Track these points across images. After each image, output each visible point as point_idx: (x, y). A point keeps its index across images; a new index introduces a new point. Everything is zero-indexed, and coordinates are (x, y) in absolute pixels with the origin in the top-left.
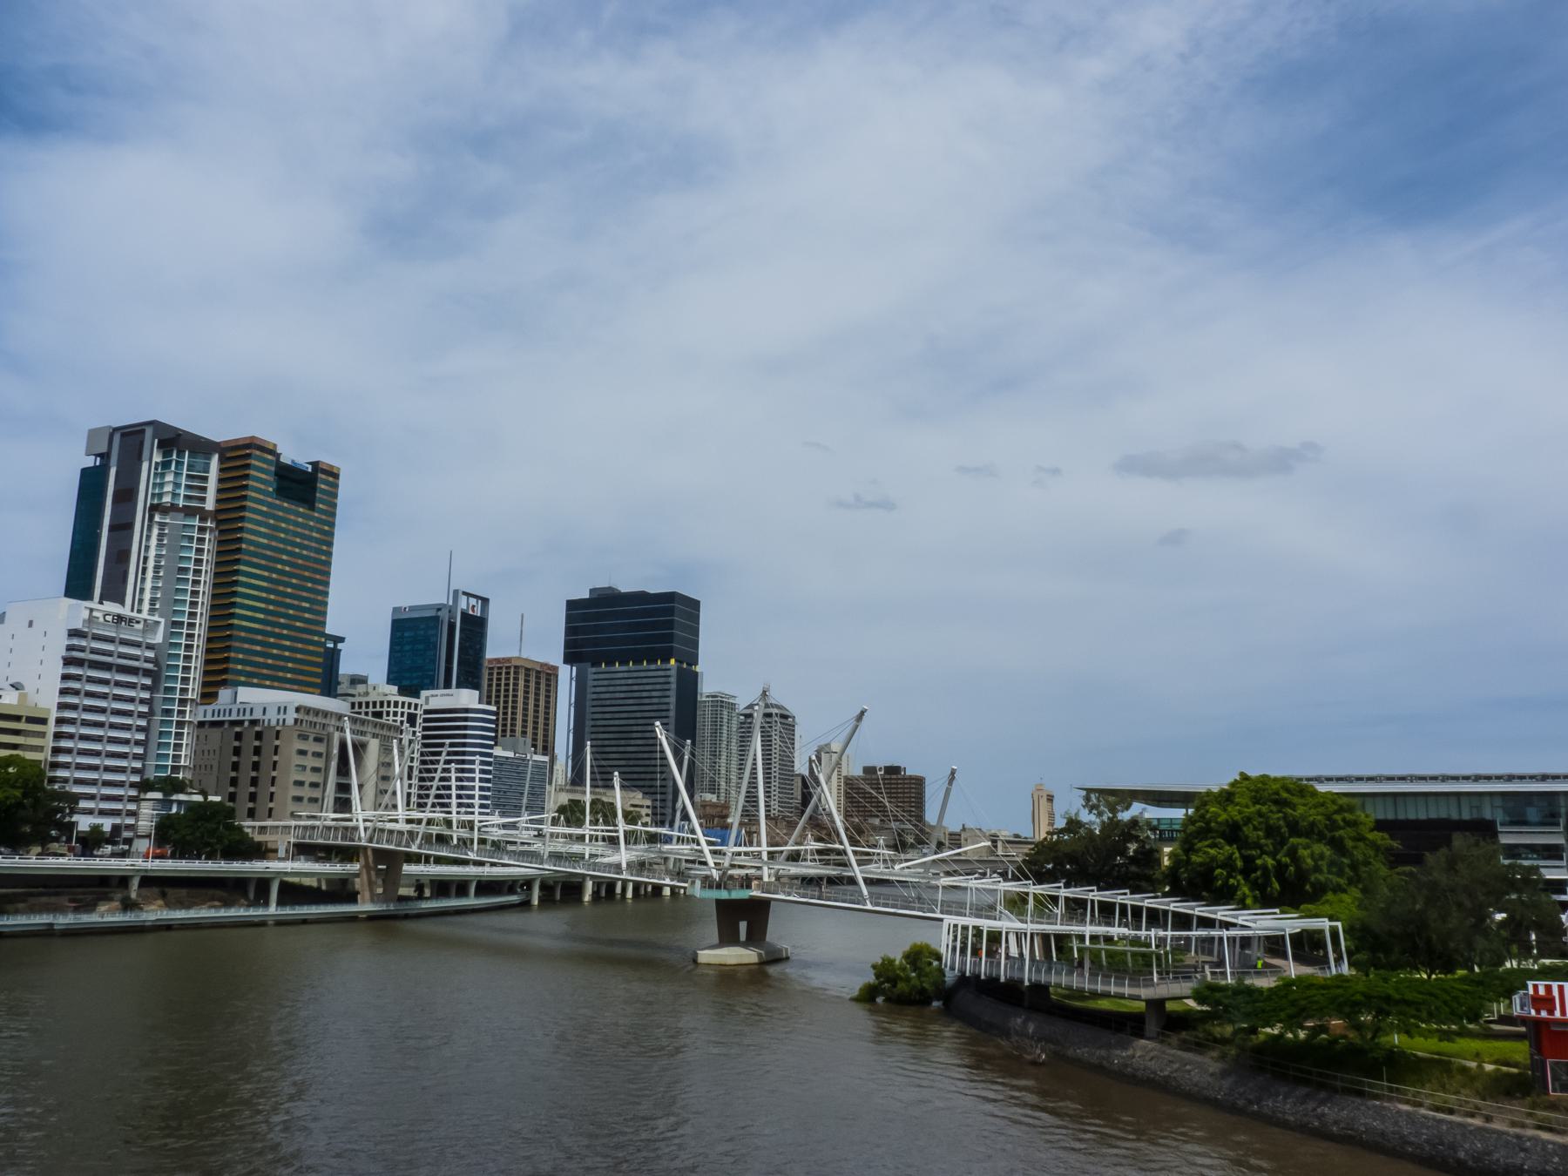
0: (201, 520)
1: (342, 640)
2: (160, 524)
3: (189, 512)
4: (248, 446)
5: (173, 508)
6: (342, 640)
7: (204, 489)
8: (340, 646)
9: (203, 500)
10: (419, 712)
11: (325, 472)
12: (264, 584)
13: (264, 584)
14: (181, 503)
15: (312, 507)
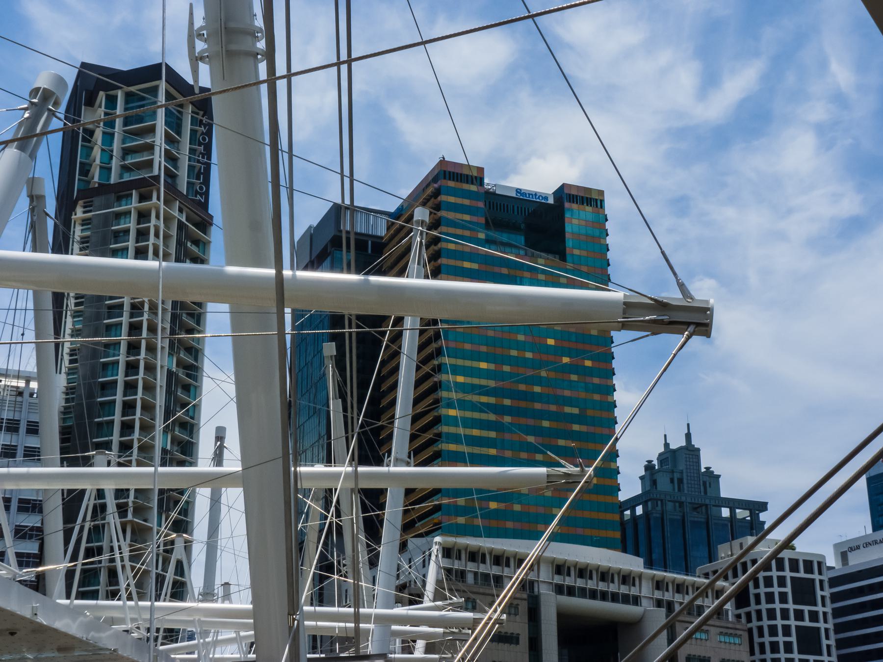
0: (143, 198)
1: (763, 506)
2: (85, 222)
3: (121, 192)
4: (435, 179)
5: (104, 189)
6: (763, 506)
7: (150, 148)
8: (763, 516)
9: (149, 164)
10: (816, 576)
11: (573, 198)
12: (492, 383)
13: (492, 383)
14: (113, 180)
15: (563, 258)
